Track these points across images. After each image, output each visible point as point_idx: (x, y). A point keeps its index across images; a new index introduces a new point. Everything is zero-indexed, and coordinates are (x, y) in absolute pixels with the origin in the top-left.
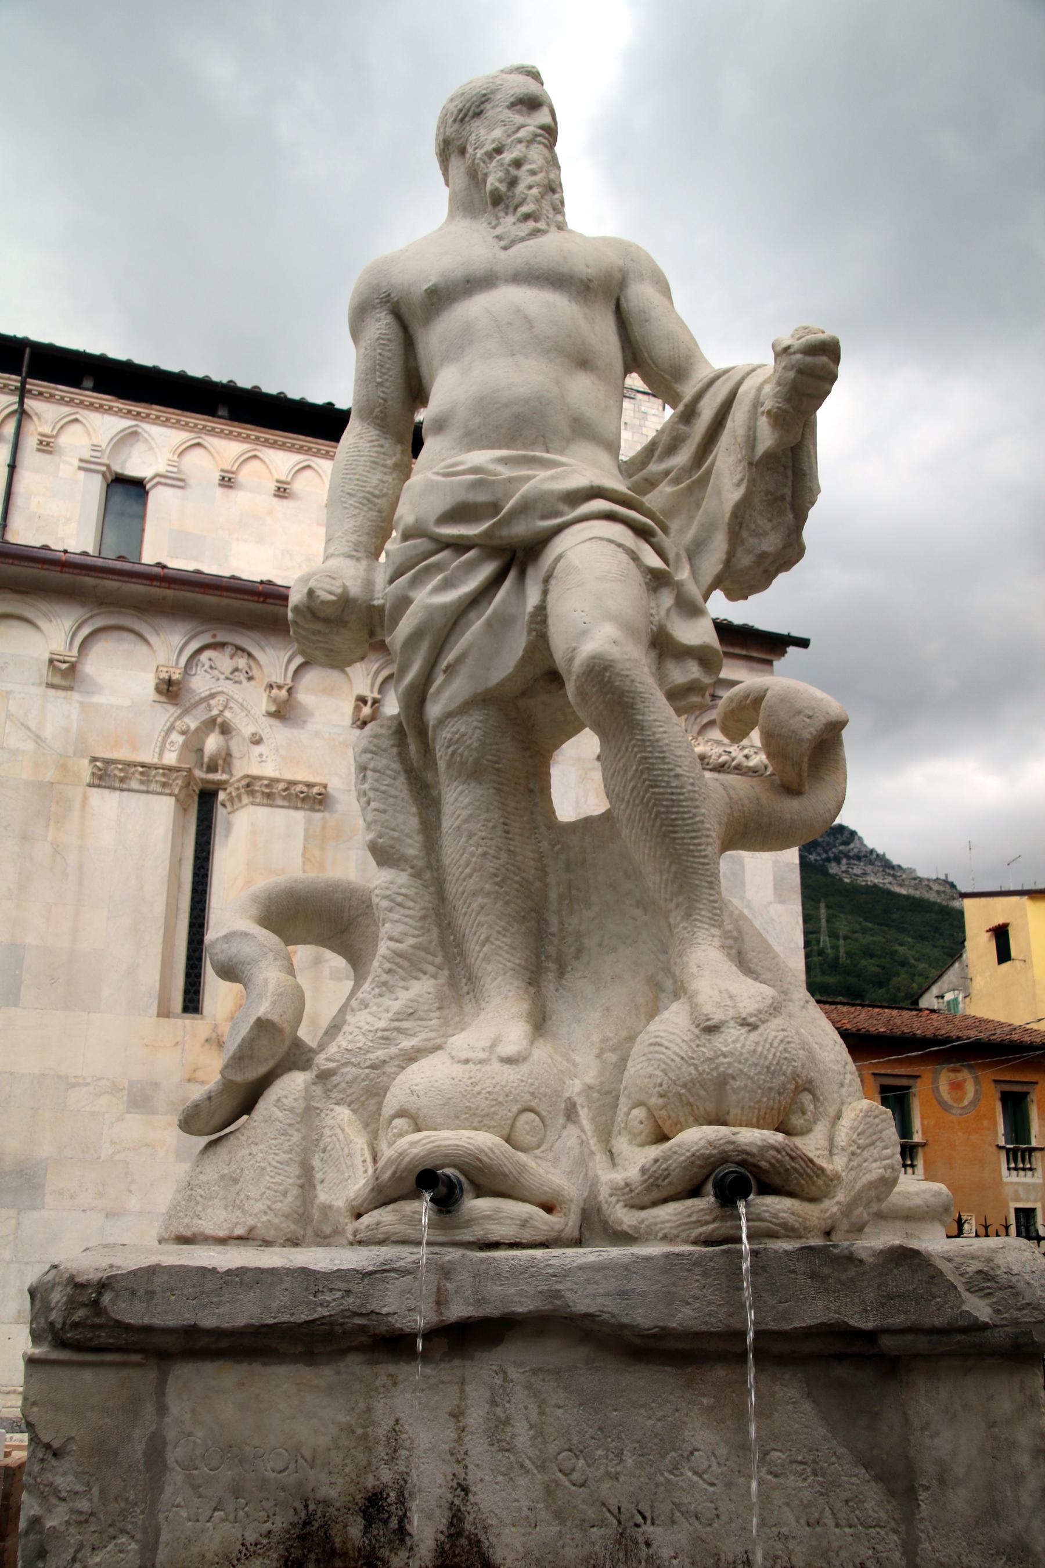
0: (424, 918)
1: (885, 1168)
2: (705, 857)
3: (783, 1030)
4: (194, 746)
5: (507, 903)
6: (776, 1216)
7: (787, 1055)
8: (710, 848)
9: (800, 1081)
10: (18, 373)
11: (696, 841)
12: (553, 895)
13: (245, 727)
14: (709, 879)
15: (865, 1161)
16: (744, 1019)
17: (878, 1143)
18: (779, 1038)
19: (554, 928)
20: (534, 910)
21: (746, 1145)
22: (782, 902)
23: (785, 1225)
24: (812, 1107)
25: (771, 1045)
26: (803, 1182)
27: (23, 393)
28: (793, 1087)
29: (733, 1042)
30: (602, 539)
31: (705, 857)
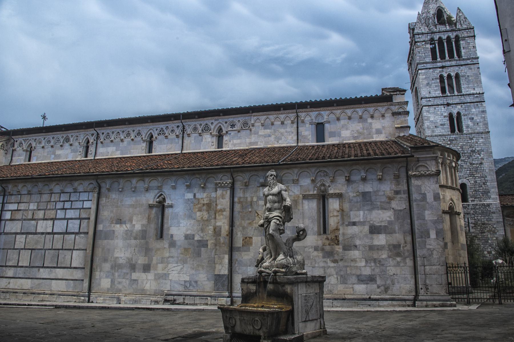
4: (319, 189)
10: (295, 109)
13: (327, 185)
22: (436, 201)
27: (297, 112)
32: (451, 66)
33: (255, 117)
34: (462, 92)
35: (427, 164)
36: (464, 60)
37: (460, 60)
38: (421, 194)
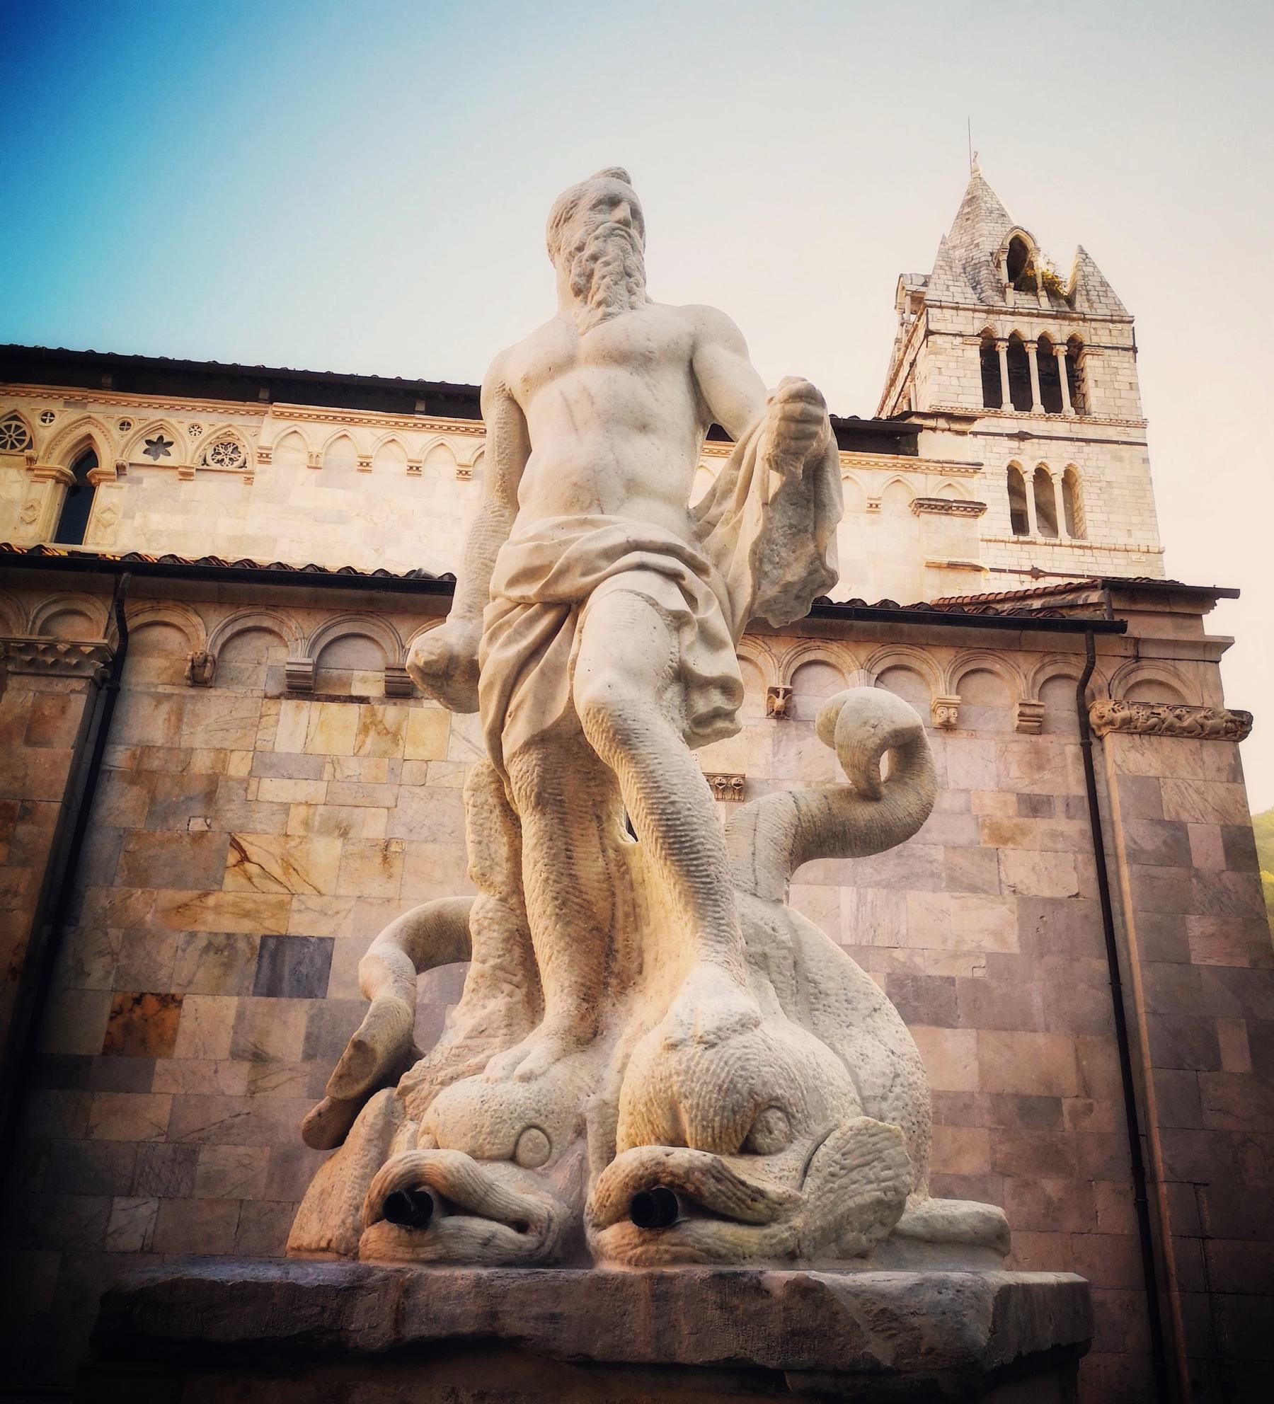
0: (506, 940)
1: (885, 1191)
2: (708, 876)
3: (745, 1047)
5: (568, 924)
6: (699, 1241)
7: (743, 1073)
8: (712, 868)
9: (760, 1100)
11: (695, 862)
12: (620, 914)
14: (713, 897)
15: (854, 1183)
16: (701, 1037)
17: (876, 1163)
18: (738, 1055)
19: (619, 945)
20: (597, 929)
21: (673, 1166)
23: (708, 1251)
24: (781, 1125)
25: (726, 1063)
26: (732, 1205)
28: (751, 1105)
29: (688, 1060)
30: (622, 590)
31: (708, 876)
32: (1051, 438)
33: (284, 425)
34: (1082, 537)
35: (1178, 676)
36: (1095, 423)
37: (1081, 422)
38: (1161, 823)
